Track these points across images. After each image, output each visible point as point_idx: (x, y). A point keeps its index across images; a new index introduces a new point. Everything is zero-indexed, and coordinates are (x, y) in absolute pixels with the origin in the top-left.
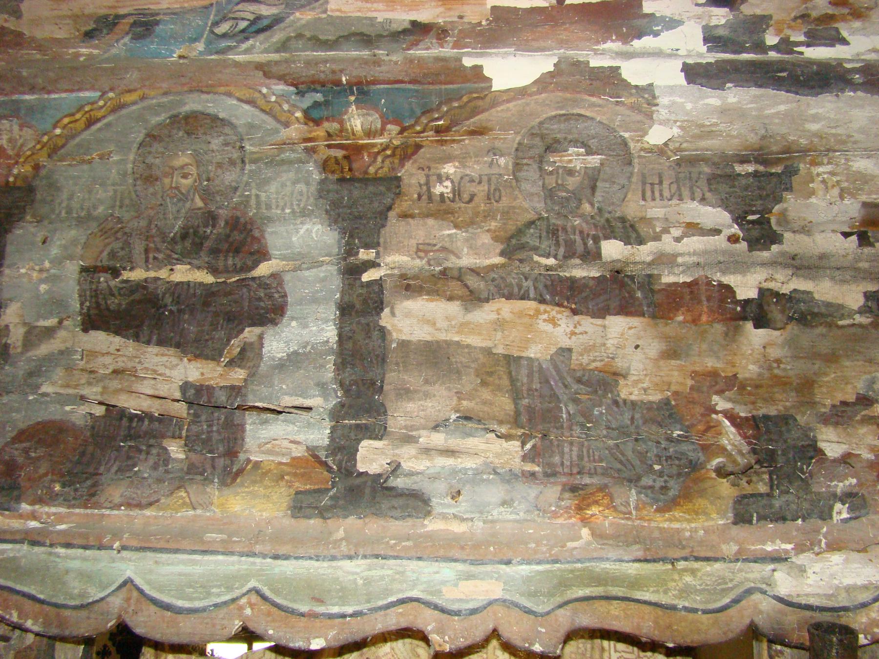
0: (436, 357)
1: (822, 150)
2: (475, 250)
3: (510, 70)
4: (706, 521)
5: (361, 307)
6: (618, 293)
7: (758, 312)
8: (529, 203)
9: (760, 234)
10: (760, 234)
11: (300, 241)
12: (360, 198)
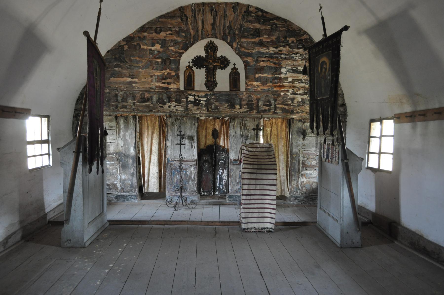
0: (278, 107)
1: (296, 98)
2: (280, 103)
3: (282, 94)
4: (289, 114)
5: (275, 105)
6: (286, 105)
7: (292, 106)
8: (282, 100)
9: (293, 102)
10: (293, 102)
11: (273, 102)
12: (275, 100)
